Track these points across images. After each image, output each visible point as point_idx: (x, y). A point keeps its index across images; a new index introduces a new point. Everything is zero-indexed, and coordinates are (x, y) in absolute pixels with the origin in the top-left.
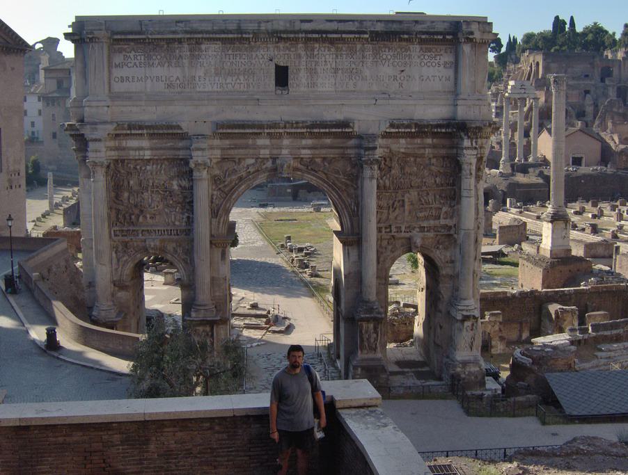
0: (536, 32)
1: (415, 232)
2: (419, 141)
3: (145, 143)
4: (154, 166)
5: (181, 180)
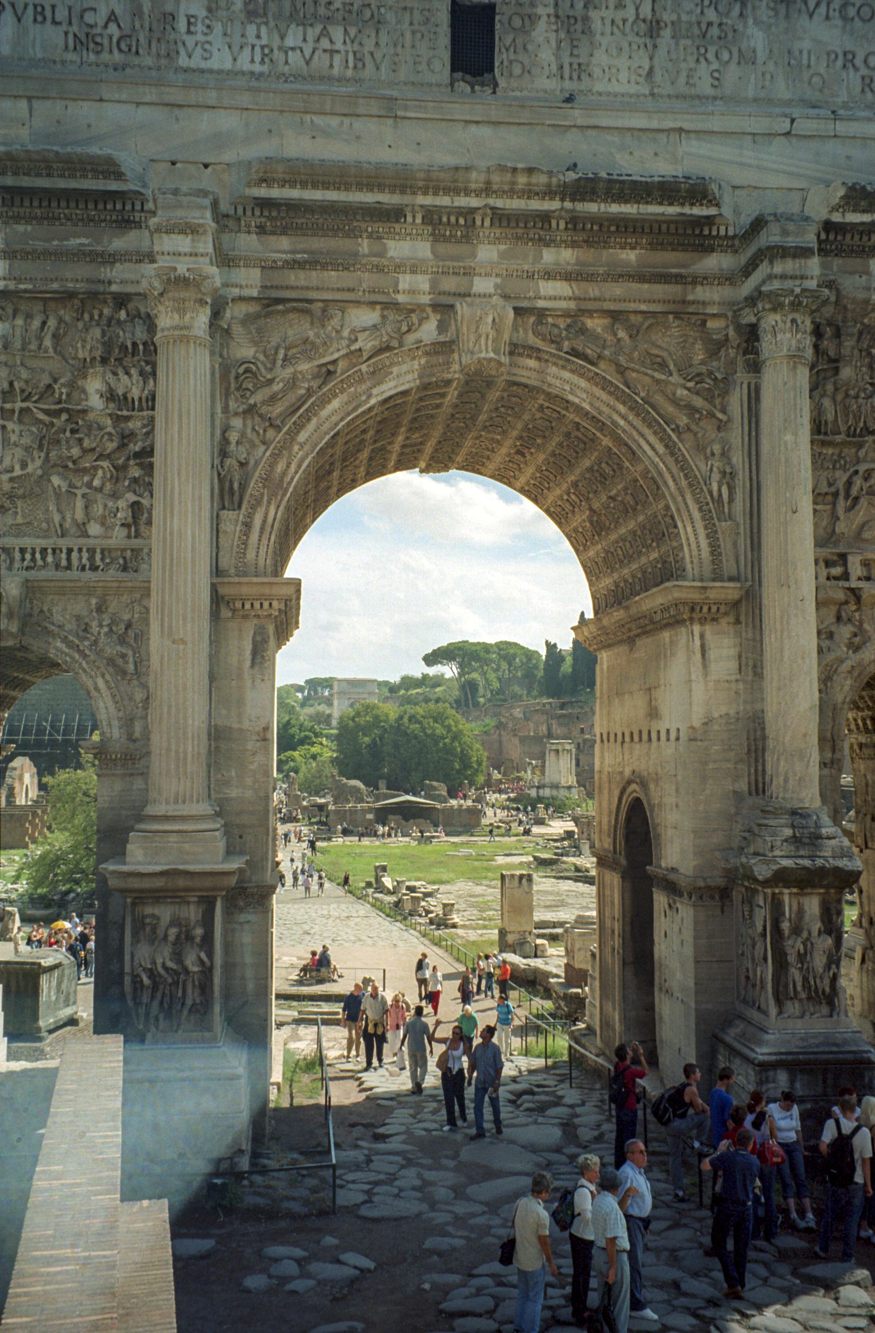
4: (19, 322)
5: (115, 374)
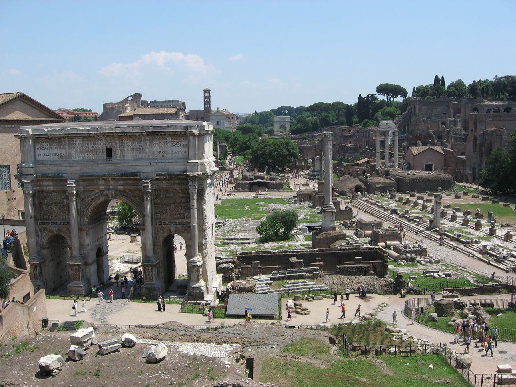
0: (424, 85)
2: (172, 182)
3: (51, 183)
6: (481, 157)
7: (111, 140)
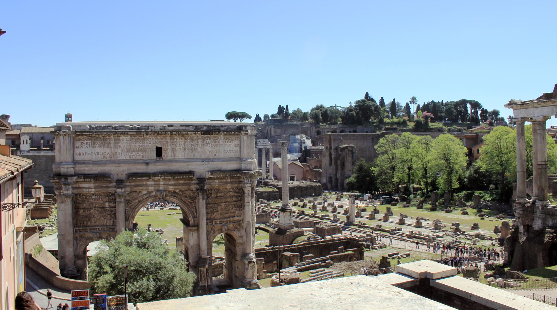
1: (223, 223)
2: (224, 180)
3: (92, 185)
4: (96, 197)
6: (337, 169)
7: (162, 139)
